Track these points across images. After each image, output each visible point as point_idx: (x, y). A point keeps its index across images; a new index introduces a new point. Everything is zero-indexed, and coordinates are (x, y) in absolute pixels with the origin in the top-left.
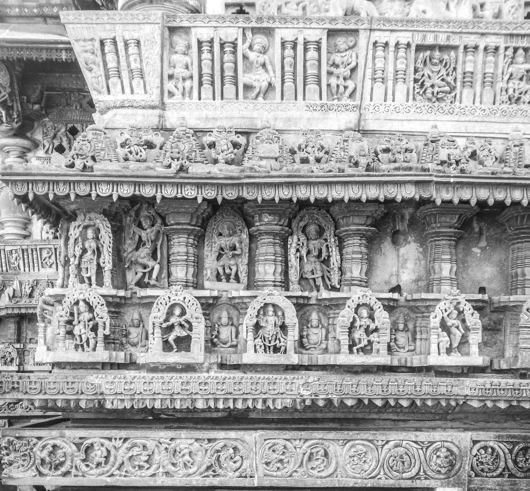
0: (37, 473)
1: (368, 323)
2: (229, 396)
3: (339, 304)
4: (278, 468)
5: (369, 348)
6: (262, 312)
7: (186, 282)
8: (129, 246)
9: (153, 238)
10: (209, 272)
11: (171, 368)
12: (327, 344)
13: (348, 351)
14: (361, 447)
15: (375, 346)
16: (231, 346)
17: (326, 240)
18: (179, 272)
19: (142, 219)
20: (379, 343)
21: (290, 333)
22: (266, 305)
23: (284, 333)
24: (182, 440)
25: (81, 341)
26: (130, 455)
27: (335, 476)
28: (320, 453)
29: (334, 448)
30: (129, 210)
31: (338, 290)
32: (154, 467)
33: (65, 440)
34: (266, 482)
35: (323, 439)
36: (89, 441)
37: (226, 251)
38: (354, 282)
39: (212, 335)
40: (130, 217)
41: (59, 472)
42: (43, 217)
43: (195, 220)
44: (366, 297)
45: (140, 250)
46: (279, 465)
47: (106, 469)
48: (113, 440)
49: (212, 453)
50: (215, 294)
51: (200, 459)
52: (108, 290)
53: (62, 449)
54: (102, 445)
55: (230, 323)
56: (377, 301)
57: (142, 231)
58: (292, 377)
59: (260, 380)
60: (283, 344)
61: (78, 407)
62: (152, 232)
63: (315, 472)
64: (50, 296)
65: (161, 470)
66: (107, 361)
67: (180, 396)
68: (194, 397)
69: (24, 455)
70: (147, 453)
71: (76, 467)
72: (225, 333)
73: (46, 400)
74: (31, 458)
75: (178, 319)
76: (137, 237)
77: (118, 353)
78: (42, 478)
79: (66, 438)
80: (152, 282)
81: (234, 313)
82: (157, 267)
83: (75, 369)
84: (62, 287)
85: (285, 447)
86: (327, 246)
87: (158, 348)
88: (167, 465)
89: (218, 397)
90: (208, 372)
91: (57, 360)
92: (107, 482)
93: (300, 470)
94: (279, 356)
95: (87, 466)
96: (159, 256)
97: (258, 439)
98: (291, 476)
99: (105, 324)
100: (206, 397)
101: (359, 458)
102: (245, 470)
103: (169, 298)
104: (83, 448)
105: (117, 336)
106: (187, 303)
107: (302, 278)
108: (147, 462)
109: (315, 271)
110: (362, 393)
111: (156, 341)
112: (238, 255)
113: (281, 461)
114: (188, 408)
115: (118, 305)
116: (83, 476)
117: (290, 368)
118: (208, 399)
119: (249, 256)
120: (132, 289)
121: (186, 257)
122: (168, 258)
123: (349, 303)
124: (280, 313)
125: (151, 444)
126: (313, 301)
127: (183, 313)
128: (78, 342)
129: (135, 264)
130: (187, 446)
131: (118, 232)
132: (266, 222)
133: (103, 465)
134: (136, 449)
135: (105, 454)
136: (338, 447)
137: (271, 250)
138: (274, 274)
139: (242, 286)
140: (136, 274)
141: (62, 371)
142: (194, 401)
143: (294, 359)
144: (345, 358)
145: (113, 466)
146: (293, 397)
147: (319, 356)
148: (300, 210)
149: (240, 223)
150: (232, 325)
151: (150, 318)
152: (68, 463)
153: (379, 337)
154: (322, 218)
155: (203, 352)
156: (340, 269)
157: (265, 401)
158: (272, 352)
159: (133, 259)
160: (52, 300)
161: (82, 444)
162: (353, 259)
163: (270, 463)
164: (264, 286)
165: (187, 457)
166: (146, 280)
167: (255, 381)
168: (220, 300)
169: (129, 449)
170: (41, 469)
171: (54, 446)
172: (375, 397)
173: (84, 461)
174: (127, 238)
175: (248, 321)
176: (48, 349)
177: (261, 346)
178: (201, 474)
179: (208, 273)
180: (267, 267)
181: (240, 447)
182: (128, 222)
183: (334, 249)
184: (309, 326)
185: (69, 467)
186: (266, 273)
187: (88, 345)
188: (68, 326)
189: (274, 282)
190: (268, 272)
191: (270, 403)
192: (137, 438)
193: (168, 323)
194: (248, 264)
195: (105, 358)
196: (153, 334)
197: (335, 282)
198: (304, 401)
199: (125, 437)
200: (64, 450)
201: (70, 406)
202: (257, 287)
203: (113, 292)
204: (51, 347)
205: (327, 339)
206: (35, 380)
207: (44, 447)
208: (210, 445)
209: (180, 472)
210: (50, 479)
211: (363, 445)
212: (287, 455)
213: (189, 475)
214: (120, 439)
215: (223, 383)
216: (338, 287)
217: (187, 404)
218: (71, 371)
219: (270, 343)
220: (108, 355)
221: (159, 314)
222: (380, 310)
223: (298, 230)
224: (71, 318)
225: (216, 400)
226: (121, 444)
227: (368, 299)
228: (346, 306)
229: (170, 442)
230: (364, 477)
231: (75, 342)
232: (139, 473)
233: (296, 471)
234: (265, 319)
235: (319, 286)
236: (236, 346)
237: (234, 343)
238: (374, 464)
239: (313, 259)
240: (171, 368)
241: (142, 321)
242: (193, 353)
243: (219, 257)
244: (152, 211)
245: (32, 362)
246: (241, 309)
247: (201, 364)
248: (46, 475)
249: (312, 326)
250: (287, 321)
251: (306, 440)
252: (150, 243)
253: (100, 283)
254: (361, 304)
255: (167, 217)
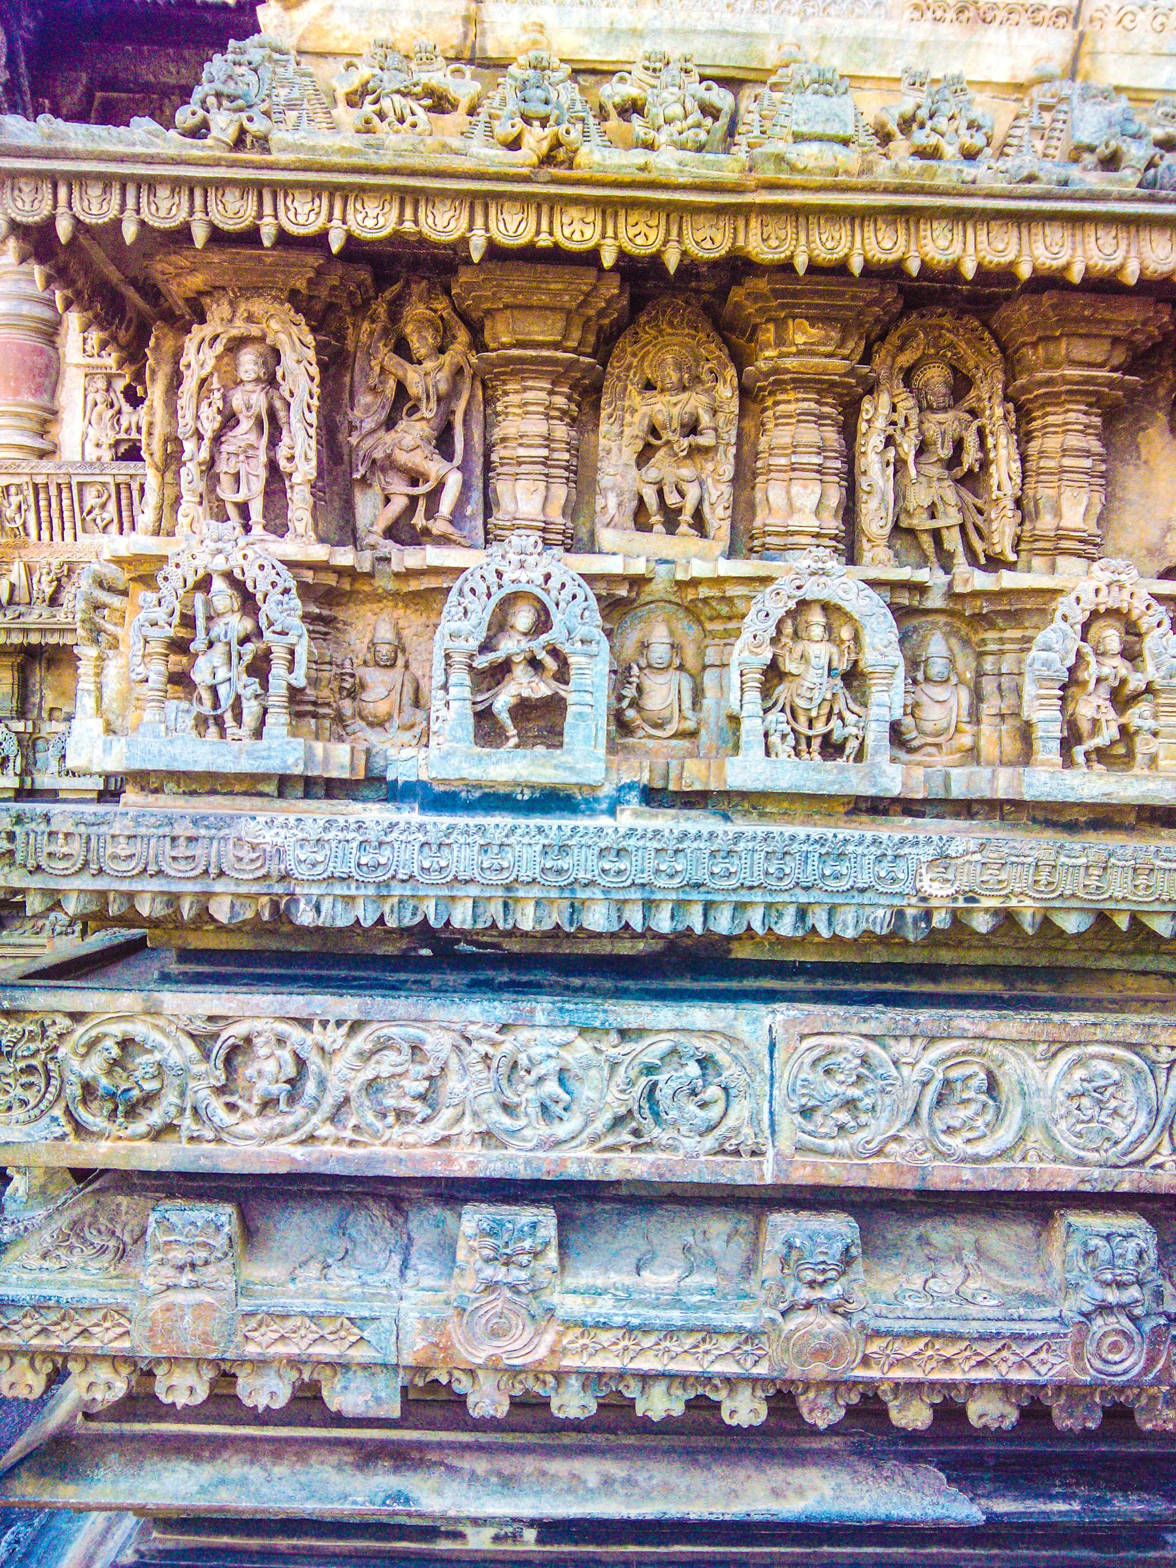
0: (68, 1129)
1: (1123, 672)
2: (694, 895)
3: (1023, 610)
4: (841, 1127)
5: (1121, 750)
6: (788, 629)
7: (544, 530)
8: (366, 410)
9: (443, 387)
10: (612, 501)
11: (496, 800)
12: (976, 736)
13: (1059, 760)
14: (1103, 1066)
15: (1143, 746)
16: (678, 735)
17: (974, 413)
18: (524, 498)
19: (409, 329)
20: (1155, 734)
21: (877, 695)
22: (803, 604)
23: (855, 700)
24: (536, 1033)
25: (216, 704)
26: (369, 1074)
27: (1018, 1155)
28: (975, 1083)
29: (1016, 1067)
30: (366, 303)
31: (1011, 566)
32: (447, 1114)
33: (161, 1022)
34: (801, 1172)
35: (983, 1038)
36: (239, 1030)
37: (666, 435)
38: (1065, 544)
39: (620, 698)
40: (373, 321)
41: (140, 1127)
42: (100, 322)
43: (576, 334)
44: (1121, 587)
45: (402, 425)
46: (843, 1117)
47: (290, 1120)
48: (317, 1027)
49: (632, 1074)
50: (638, 567)
51: (593, 1095)
52: (303, 544)
53: (150, 1052)
54: (281, 1041)
55: (677, 662)
56: (1153, 602)
57: (407, 365)
58: (897, 837)
59: (795, 846)
60: (854, 731)
61: (204, 917)
62: (440, 369)
63: (956, 1142)
64: (119, 561)
65: (468, 1125)
66: (298, 770)
67: (536, 892)
68: (581, 894)
69: (30, 1070)
70: (424, 1070)
71: (195, 1110)
72: (661, 692)
73: (103, 894)
74: (49, 1078)
75: (525, 644)
76: (392, 384)
77: (330, 745)
78: (87, 1146)
79: (161, 1018)
80: (439, 527)
81: (688, 632)
82: (454, 481)
83: (192, 793)
84: (157, 533)
85: (864, 1060)
86: (981, 432)
87: (460, 733)
88: (489, 1110)
89: (658, 896)
90: (612, 812)
91: (137, 766)
92: (294, 1160)
93: (913, 1135)
94: (842, 770)
95: (232, 1107)
96: (459, 446)
97: (779, 1033)
98: (879, 1152)
99: (292, 653)
100: (621, 896)
101: (1099, 1101)
102: (737, 1130)
103: (499, 575)
104: (219, 1050)
105: (326, 693)
106: (554, 593)
107: (896, 528)
108: (422, 1097)
109: (940, 507)
110: (1119, 895)
111: (452, 711)
112: (704, 451)
113: (850, 1104)
114: (558, 926)
115: (330, 597)
116: (219, 1140)
117: (863, 806)
118: (625, 901)
119: (737, 457)
120: (373, 547)
121: (544, 452)
122: (487, 456)
123: (1063, 605)
124: (846, 633)
125: (438, 1042)
126: (935, 600)
127: (543, 623)
128: (207, 709)
129: (383, 470)
130: (553, 1051)
131: (334, 365)
132: (802, 345)
133: (283, 1106)
134: (391, 1056)
135: (291, 1071)
136: (1030, 1062)
137: (809, 434)
138: (817, 512)
139: (721, 543)
140: (387, 500)
141: (151, 798)
142: (575, 908)
143: (891, 777)
144: (1046, 780)
145: (314, 1111)
146: (897, 901)
147: (954, 772)
148: (902, 314)
149: (714, 352)
150: (681, 668)
151: (437, 637)
152: (171, 1097)
153: (1155, 717)
154: (968, 342)
155: (602, 751)
156: (1018, 503)
157: (802, 913)
158: (817, 757)
159: (378, 455)
160: (121, 577)
161: (215, 1036)
162: (1063, 470)
163: (813, 1109)
164: (785, 548)
165: (552, 1087)
166: (419, 520)
167: (777, 846)
168: (647, 589)
169: (365, 1057)
170: (83, 1114)
171: (126, 1043)
172: (1156, 907)
173: (221, 1090)
174: (360, 388)
175: (748, 652)
176: (109, 729)
177: (784, 737)
178: (595, 1139)
179: (611, 503)
180: (796, 488)
181: (722, 1058)
182: (364, 338)
183: (1003, 440)
184: (920, 676)
185: (173, 1111)
186: (791, 508)
187: (238, 718)
188: (173, 658)
189: (817, 536)
190: (798, 503)
191: (818, 919)
192: (391, 1020)
193: (491, 656)
194: (734, 481)
195: (291, 761)
196: (445, 687)
197: (1002, 542)
198: (928, 915)
199: (355, 1016)
200: (157, 1056)
201: (178, 910)
202: (763, 552)
203: (319, 553)
204: (117, 725)
205: (975, 718)
206: (69, 827)
207: (92, 1045)
208: (626, 1048)
209: (527, 1132)
210: (114, 1150)
211: (1111, 1059)
212: (869, 1086)
213: (558, 1143)
214: (339, 1023)
215: (677, 851)
216: (1012, 557)
217: (557, 916)
218: (181, 801)
219: (810, 727)
220: (300, 753)
221: (465, 626)
222: (1158, 632)
223: (890, 378)
224: (183, 633)
225: (649, 905)
226: (340, 1041)
227: (1125, 594)
228: (1058, 615)
229: (500, 1038)
230: (1114, 1160)
231: (196, 708)
232: (397, 1133)
233: (896, 1138)
234: (799, 648)
235: (951, 555)
236: (693, 734)
237: (690, 725)
238: (1142, 1119)
239: (935, 471)
240: (496, 800)
241: (404, 650)
242: (570, 752)
243: (645, 456)
244: (441, 305)
245: (54, 766)
246: (711, 619)
247: (593, 788)
248: (100, 1135)
249: (927, 679)
250: (869, 659)
251: (932, 1039)
252: (433, 404)
253: (278, 525)
254: (1102, 609)
255: (488, 323)
